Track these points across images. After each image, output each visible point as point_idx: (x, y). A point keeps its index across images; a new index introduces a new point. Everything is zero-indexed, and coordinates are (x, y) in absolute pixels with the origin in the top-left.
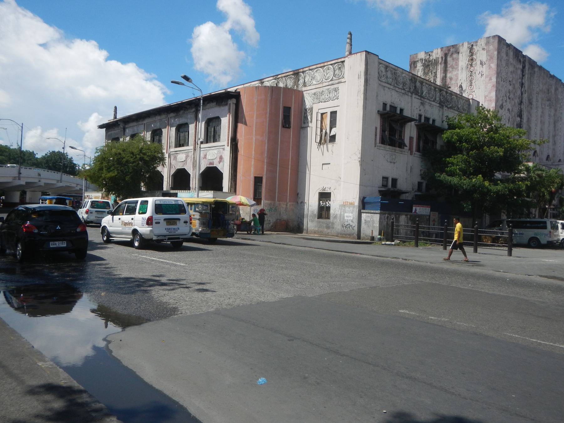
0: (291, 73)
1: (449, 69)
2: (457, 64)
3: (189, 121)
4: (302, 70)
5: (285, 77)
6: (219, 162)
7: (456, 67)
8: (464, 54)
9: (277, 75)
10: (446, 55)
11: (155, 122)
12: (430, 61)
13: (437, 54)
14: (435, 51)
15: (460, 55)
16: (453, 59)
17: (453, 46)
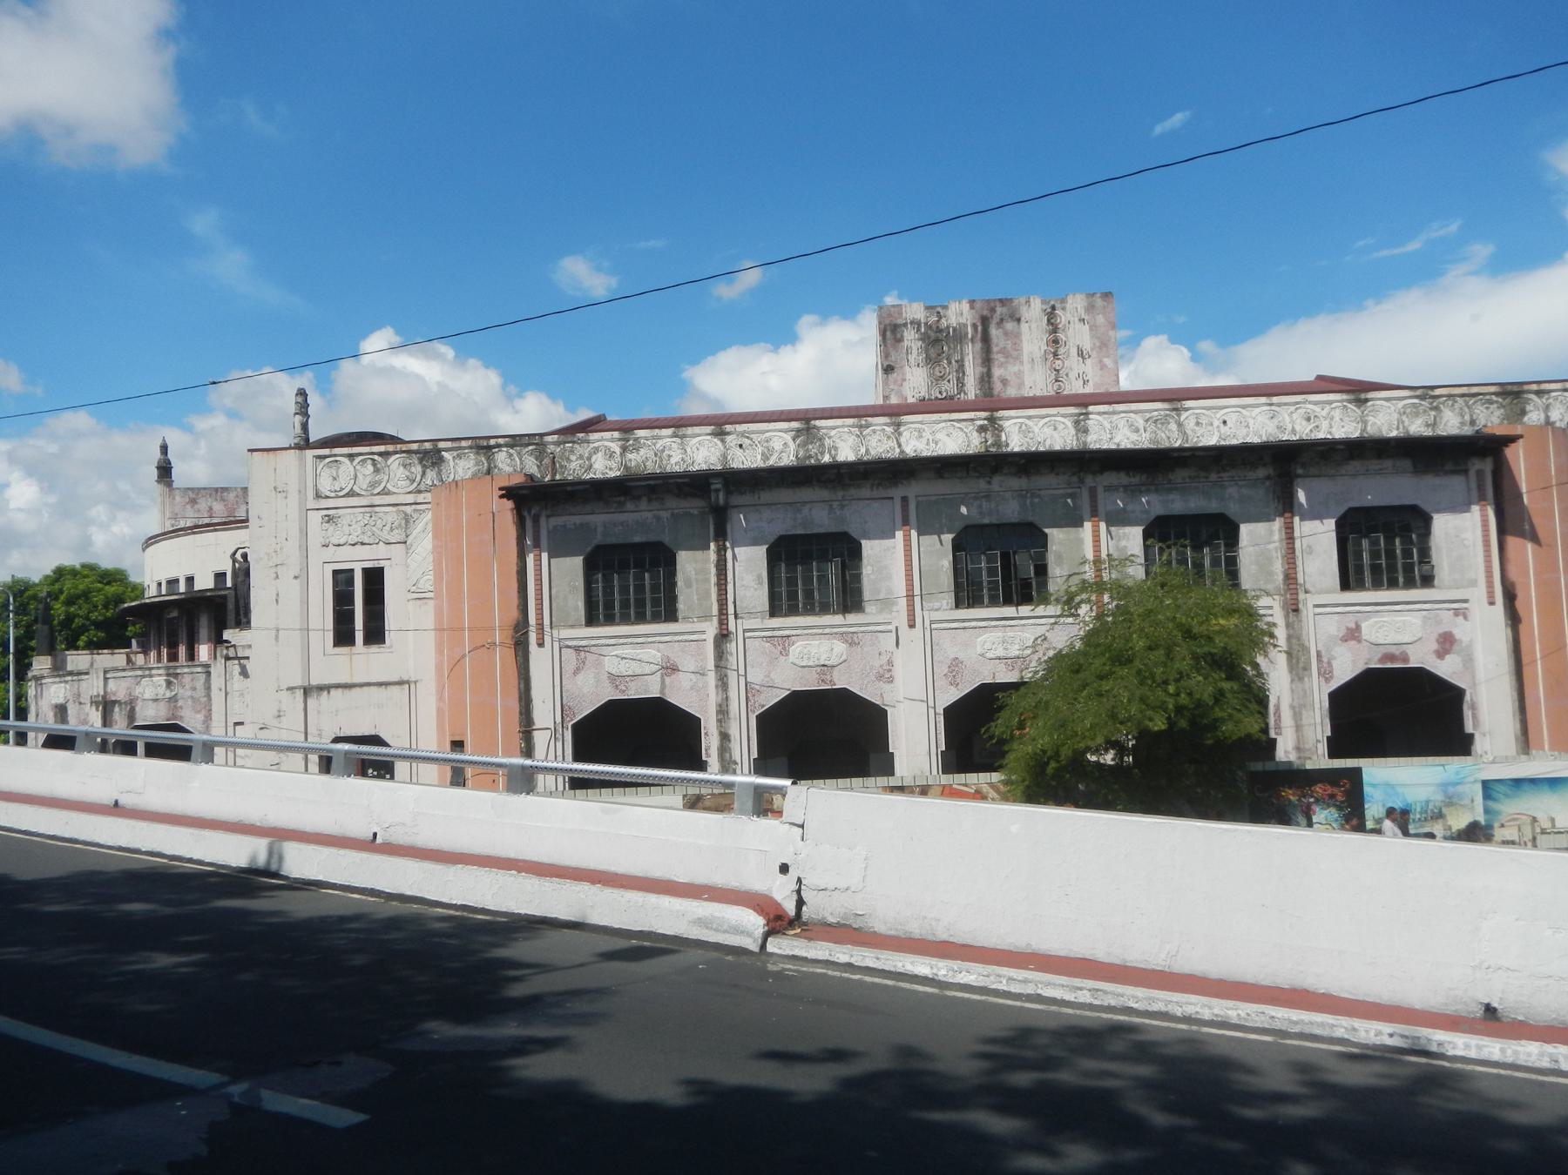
0: (1493, 389)
1: (998, 358)
2: (1017, 346)
3: (1232, 509)
4: (1534, 387)
5: (1463, 395)
6: (1441, 655)
7: (1014, 353)
8: (1034, 326)
9: (1433, 388)
10: (985, 321)
11: (988, 497)
12: (940, 331)
13: (959, 314)
14: (954, 307)
15: (1024, 327)
16: (1006, 334)
17: (1001, 301)
